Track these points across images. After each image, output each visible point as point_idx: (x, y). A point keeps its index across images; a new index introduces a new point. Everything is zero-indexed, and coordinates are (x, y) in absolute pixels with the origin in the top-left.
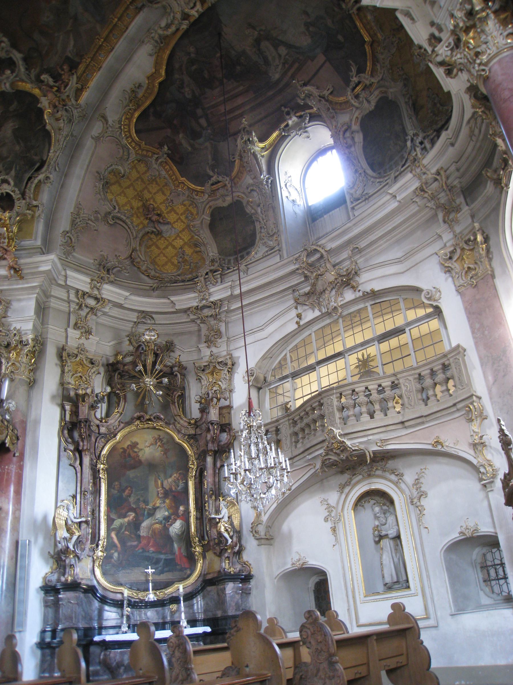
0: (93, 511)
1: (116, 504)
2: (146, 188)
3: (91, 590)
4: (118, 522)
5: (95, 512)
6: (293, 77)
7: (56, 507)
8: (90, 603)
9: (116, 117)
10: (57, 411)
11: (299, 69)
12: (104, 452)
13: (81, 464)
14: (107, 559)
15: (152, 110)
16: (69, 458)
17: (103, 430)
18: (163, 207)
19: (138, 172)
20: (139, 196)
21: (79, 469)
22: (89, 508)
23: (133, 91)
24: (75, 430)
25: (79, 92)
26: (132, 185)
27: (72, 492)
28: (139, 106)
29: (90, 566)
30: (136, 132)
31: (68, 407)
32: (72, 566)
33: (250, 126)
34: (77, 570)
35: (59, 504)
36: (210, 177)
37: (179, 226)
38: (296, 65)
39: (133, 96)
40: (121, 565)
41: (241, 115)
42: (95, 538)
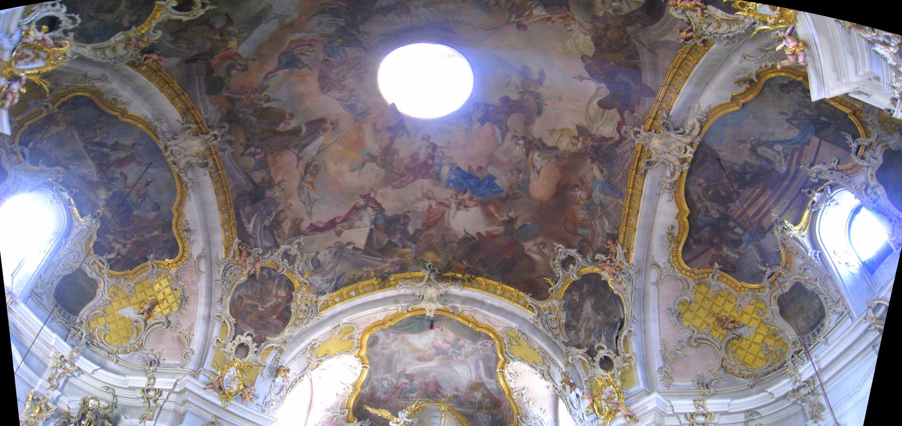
2: (714, 303)
6: (798, 163)
9: (665, 260)
11: (800, 156)
15: (691, 240)
18: (734, 314)
19: (702, 294)
20: (711, 313)
23: (669, 234)
25: (627, 255)
26: (701, 306)
28: (679, 243)
30: (686, 263)
33: (781, 216)
36: (764, 273)
37: (754, 324)
38: (796, 154)
39: (671, 238)
41: (769, 211)
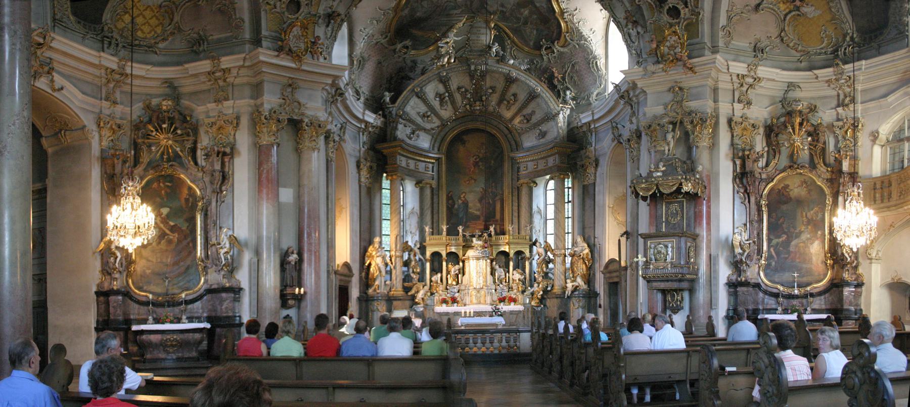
0: (758, 234)
1: (773, 228)
3: (757, 286)
4: (775, 242)
5: (760, 235)
7: (734, 234)
8: (757, 294)
10: (731, 164)
12: (765, 192)
13: (749, 202)
14: (768, 266)
16: (741, 198)
17: (764, 176)
21: (748, 205)
22: (755, 232)
24: (744, 177)
27: (744, 222)
29: (757, 270)
31: (738, 162)
32: (744, 271)
34: (748, 274)
35: (736, 231)
40: (776, 270)
42: (760, 252)
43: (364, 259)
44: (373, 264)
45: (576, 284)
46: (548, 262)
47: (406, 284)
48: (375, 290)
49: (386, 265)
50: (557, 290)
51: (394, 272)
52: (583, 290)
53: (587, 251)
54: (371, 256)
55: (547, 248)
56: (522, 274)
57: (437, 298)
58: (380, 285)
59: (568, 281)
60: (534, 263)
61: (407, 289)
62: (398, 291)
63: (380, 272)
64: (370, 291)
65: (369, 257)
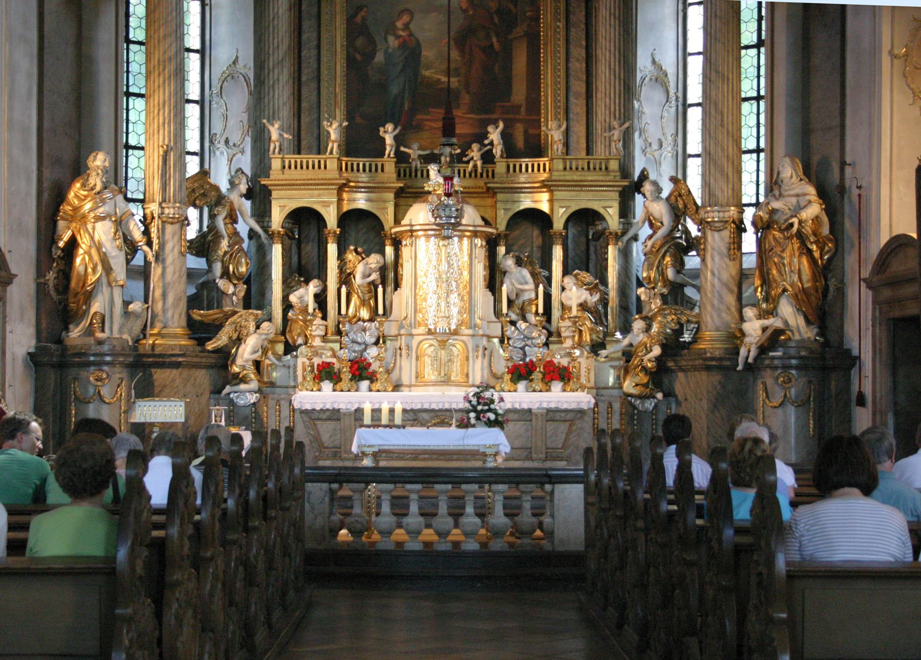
43: (55, 223)
44: (84, 242)
45: (773, 322)
46: (680, 247)
47: (197, 315)
48: (89, 332)
49: (131, 248)
50: (711, 342)
51: (156, 272)
52: (802, 344)
53: (814, 209)
54: (78, 217)
55: (680, 205)
56: (592, 289)
57: (302, 360)
58: (109, 310)
59: (749, 312)
60: (637, 249)
61: (200, 331)
62: (170, 332)
63: (108, 269)
64: (75, 333)
65: (71, 219)
